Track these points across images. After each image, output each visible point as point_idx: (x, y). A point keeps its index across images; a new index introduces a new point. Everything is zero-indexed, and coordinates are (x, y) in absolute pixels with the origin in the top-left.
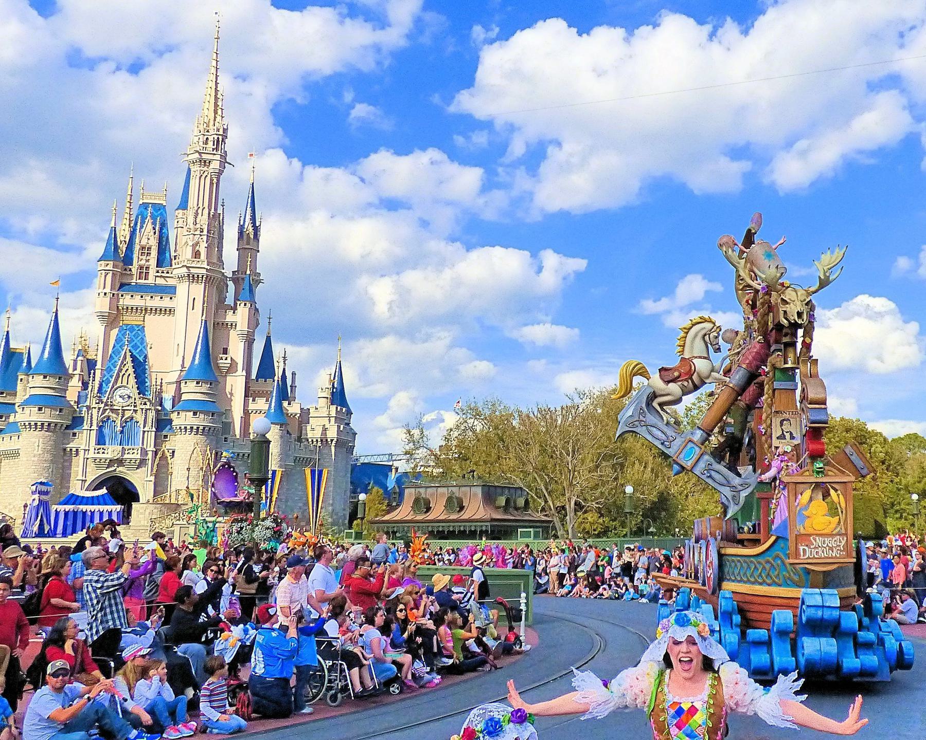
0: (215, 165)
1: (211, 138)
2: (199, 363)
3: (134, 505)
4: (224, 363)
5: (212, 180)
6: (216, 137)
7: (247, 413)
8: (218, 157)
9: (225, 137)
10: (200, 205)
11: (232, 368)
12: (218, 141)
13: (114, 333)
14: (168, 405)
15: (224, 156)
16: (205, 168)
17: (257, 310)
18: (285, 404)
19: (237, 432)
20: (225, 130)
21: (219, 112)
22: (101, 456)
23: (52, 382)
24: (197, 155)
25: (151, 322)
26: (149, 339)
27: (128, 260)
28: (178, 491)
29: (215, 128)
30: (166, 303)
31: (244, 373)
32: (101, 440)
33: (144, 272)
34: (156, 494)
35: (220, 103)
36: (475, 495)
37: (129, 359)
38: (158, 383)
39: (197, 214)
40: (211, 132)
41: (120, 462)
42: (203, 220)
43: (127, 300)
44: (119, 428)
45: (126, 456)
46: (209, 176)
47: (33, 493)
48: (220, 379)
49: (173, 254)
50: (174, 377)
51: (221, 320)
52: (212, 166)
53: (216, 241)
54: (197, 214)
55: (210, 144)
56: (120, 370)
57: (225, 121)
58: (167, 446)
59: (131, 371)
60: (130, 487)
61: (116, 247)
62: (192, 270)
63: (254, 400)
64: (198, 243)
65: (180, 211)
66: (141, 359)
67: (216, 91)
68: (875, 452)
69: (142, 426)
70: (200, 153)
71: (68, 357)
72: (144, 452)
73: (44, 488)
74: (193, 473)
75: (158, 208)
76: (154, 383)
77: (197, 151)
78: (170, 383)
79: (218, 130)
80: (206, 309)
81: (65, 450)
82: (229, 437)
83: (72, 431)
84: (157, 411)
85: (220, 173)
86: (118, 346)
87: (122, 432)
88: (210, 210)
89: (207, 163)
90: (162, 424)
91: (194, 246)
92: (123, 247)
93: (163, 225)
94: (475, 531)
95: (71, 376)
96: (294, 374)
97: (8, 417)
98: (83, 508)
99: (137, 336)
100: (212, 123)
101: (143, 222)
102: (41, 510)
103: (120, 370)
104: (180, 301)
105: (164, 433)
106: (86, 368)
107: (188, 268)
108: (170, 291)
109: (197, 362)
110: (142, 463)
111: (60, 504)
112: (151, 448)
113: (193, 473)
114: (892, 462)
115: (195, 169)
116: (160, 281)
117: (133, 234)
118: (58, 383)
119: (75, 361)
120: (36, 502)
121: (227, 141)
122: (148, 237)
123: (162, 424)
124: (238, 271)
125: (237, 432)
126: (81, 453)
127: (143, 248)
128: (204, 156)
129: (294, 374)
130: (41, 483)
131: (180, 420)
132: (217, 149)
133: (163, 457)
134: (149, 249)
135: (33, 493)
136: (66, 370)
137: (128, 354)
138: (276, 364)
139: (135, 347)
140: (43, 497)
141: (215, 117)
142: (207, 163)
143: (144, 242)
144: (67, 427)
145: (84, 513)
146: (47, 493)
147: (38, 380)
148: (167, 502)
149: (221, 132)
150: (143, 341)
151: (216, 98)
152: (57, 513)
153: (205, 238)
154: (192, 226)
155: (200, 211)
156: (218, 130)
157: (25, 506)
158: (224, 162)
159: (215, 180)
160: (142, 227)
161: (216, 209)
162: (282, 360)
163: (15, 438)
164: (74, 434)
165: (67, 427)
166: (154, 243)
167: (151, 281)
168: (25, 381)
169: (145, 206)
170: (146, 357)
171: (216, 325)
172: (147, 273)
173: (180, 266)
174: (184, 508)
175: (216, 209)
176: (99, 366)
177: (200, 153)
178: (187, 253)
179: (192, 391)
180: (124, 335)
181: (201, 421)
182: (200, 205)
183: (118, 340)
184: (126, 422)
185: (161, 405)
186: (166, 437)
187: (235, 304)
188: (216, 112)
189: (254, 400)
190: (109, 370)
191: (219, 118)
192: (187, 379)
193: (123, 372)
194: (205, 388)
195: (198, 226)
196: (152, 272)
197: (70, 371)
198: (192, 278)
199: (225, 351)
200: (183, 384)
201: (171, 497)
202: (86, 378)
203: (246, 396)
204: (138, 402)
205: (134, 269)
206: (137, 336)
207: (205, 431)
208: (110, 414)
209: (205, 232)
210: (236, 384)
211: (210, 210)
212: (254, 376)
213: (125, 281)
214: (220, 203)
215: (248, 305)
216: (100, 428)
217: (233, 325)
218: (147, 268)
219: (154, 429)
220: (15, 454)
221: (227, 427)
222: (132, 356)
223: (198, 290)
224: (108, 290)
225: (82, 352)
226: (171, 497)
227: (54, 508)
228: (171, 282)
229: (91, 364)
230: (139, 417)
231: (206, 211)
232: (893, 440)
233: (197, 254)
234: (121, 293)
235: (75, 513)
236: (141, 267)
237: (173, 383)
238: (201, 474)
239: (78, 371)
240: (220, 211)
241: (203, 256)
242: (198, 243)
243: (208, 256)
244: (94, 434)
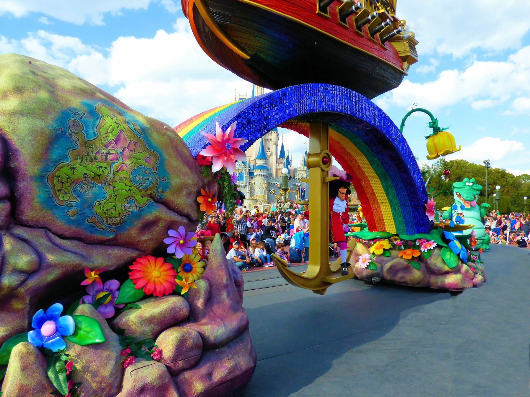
2: (261, 153)
3: (244, 200)
4: (268, 153)
7: (277, 170)
11: (271, 154)
14: (252, 167)
17: (278, 134)
18: (289, 166)
19: (274, 176)
28: (257, 196)
31: (275, 156)
34: (250, 196)
36: (355, 196)
45: (240, 184)
48: (268, 158)
50: (253, 158)
60: (242, 194)
63: (279, 165)
68: (508, 181)
72: (246, 183)
78: (252, 160)
82: (271, 178)
84: (249, 169)
87: (239, 177)
90: (251, 174)
94: (355, 209)
96: (291, 156)
109: (260, 153)
110: (245, 186)
112: (248, 182)
113: (261, 189)
114: (516, 185)
123: (251, 174)
125: (274, 176)
129: (291, 156)
131: (257, 172)
133: (252, 185)
138: (285, 153)
162: (287, 151)
179: (259, 163)
181: (263, 172)
185: (250, 167)
186: (252, 178)
189: (279, 165)
199: (269, 149)
201: (255, 197)
203: (276, 164)
204: (243, 167)
207: (264, 176)
210: (272, 160)
212: (278, 157)
215: (276, 132)
217: (271, 140)
221: (270, 175)
226: (255, 197)
230: (244, 172)
232: (517, 177)
237: (253, 160)
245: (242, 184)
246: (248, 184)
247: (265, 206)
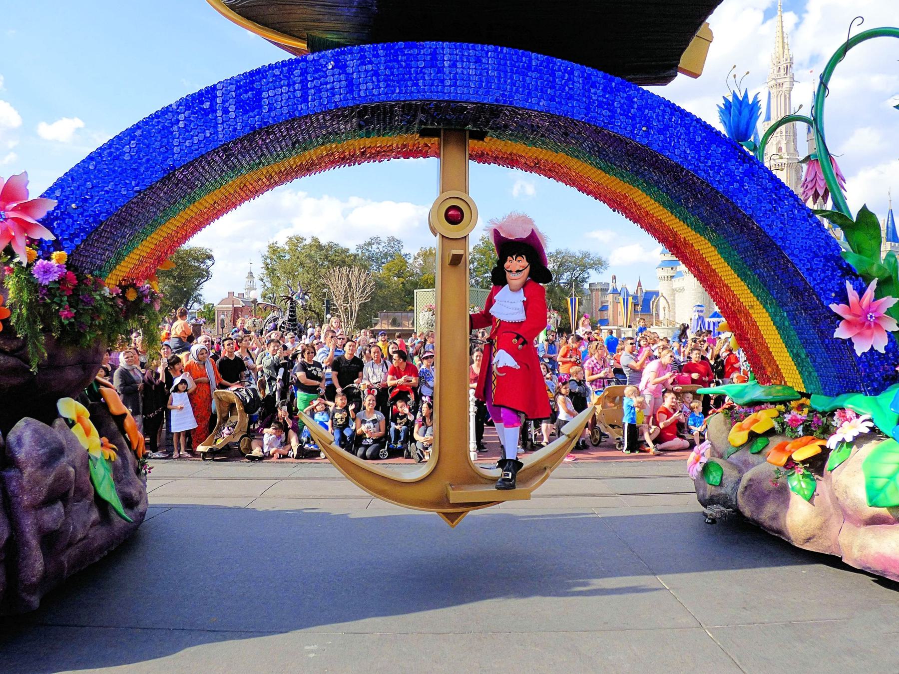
0: (787, 86)
1: (782, 67)
8: (788, 79)
15: (792, 78)
16: (780, 89)
20: (791, 59)
21: (786, 46)
35: (786, 41)
40: (782, 63)
47: (695, 311)
52: (785, 86)
55: (782, 70)
57: (791, 52)
64: (779, 142)
65: (766, 123)
67: (783, 32)
70: (775, 79)
73: (700, 309)
77: (773, 79)
79: (787, 60)
85: (791, 89)
89: (780, 85)
91: (777, 144)
97: (676, 268)
100: (782, 56)
102: (700, 322)
111: (710, 317)
120: (697, 317)
128: (779, 81)
132: (787, 73)
135: (695, 311)
140: (701, 314)
141: (784, 52)
142: (780, 85)
146: (702, 311)
149: (789, 61)
151: (783, 38)
152: (709, 323)
153: (784, 137)
156: (787, 60)
159: (788, 96)
163: (681, 280)
177: (775, 79)
188: (783, 48)
191: (786, 51)
220: (682, 290)
227: (707, 320)
233: (780, 149)
241: (784, 150)
242: (779, 142)
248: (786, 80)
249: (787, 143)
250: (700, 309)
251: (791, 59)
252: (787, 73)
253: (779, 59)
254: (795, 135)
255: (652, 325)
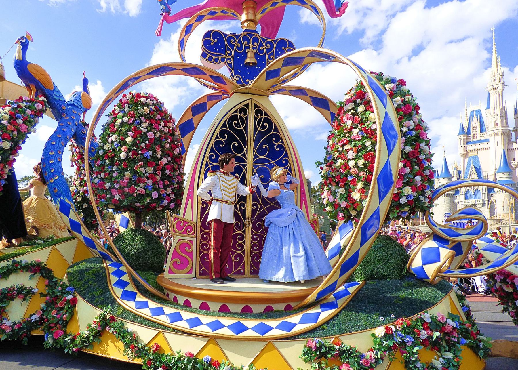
0: (500, 88)
1: (497, 79)
2: (503, 165)
5: (499, 94)
6: (499, 77)
8: (501, 85)
9: (503, 76)
10: (495, 104)
12: (500, 78)
13: (467, 160)
16: (496, 91)
22: (467, 203)
23: (446, 180)
24: (492, 87)
25: (481, 154)
26: (480, 160)
27: (468, 133)
29: (498, 74)
30: (485, 145)
32: (466, 198)
33: (475, 136)
34: (491, 216)
37: (474, 168)
38: (487, 175)
39: (494, 109)
40: (496, 76)
41: (475, 205)
42: (498, 111)
43: (470, 147)
44: (473, 193)
45: (477, 203)
46: (498, 94)
47: (445, 217)
48: (513, 171)
49: (486, 127)
50: (493, 173)
51: (510, 148)
53: (504, 118)
54: (494, 109)
55: (497, 80)
56: (471, 173)
58: (493, 198)
59: (475, 172)
61: (463, 129)
62: (495, 131)
64: (496, 120)
66: (478, 168)
69: (482, 192)
71: (451, 170)
72: (484, 201)
73: (448, 215)
74: (505, 207)
75: (479, 111)
76: (484, 176)
80: (503, 144)
81: (454, 202)
83: (455, 196)
85: (503, 90)
86: (469, 164)
87: (474, 195)
88: (500, 106)
91: (495, 122)
92: (466, 129)
93: (481, 117)
95: (453, 177)
98: (463, 221)
99: (475, 159)
101: (472, 118)
103: (471, 173)
104: (491, 144)
105: (491, 194)
106: (458, 174)
107: (493, 131)
108: (487, 140)
110: (483, 205)
112: (486, 199)
115: (492, 93)
116: (482, 138)
117: (469, 123)
118: (449, 180)
119: (454, 172)
121: (504, 77)
122: (475, 123)
124: (516, 127)
126: (460, 203)
127: (474, 127)
128: (495, 86)
130: (447, 214)
132: (500, 82)
133: (492, 202)
134: (476, 127)
136: (451, 175)
137: (473, 167)
139: (476, 163)
143: (474, 126)
144: (454, 195)
145: (464, 223)
147: (442, 180)
148: (496, 218)
149: (501, 74)
150: (478, 161)
153: (499, 118)
154: (493, 114)
155: (496, 108)
157: (443, 221)
158: (504, 85)
159: (501, 94)
160: (472, 120)
161: (503, 105)
164: (457, 197)
165: (454, 195)
166: (478, 125)
167: (478, 139)
168: (437, 181)
169: (473, 112)
170: (480, 167)
171: (508, 150)
172: (476, 136)
173: (490, 130)
174: (503, 220)
175: (503, 105)
176: (462, 173)
178: (493, 125)
179: (502, 177)
180: (471, 160)
182: (495, 104)
183: (469, 162)
184: (475, 191)
187: (516, 140)
190: (466, 173)
192: (498, 172)
193: (472, 173)
194: (507, 175)
195: (496, 114)
196: (479, 135)
197: (452, 175)
198: (496, 134)
199: (514, 160)
200: (497, 175)
202: (458, 177)
205: (471, 135)
206: (475, 159)
208: (469, 189)
209: (499, 115)
211: (500, 106)
213: (469, 141)
214: (504, 102)
216: (466, 194)
218: (476, 134)
219: (487, 192)
222: (475, 167)
223: (499, 138)
224: (462, 145)
225: (456, 168)
228: (486, 138)
229: (459, 172)
231: (498, 107)
233: (496, 125)
234: (467, 145)
235: (460, 223)
236: (474, 135)
238: (509, 208)
239: (455, 175)
240: (504, 105)
243: (502, 124)
244: (464, 196)
245: (478, 203)
246: (486, 202)
247: (512, 227)
248: (499, 85)
249: (502, 121)
250: (448, 215)
251: (502, 73)
252: (500, 82)
253: (495, 74)
254: (506, 115)
255: (420, 224)
